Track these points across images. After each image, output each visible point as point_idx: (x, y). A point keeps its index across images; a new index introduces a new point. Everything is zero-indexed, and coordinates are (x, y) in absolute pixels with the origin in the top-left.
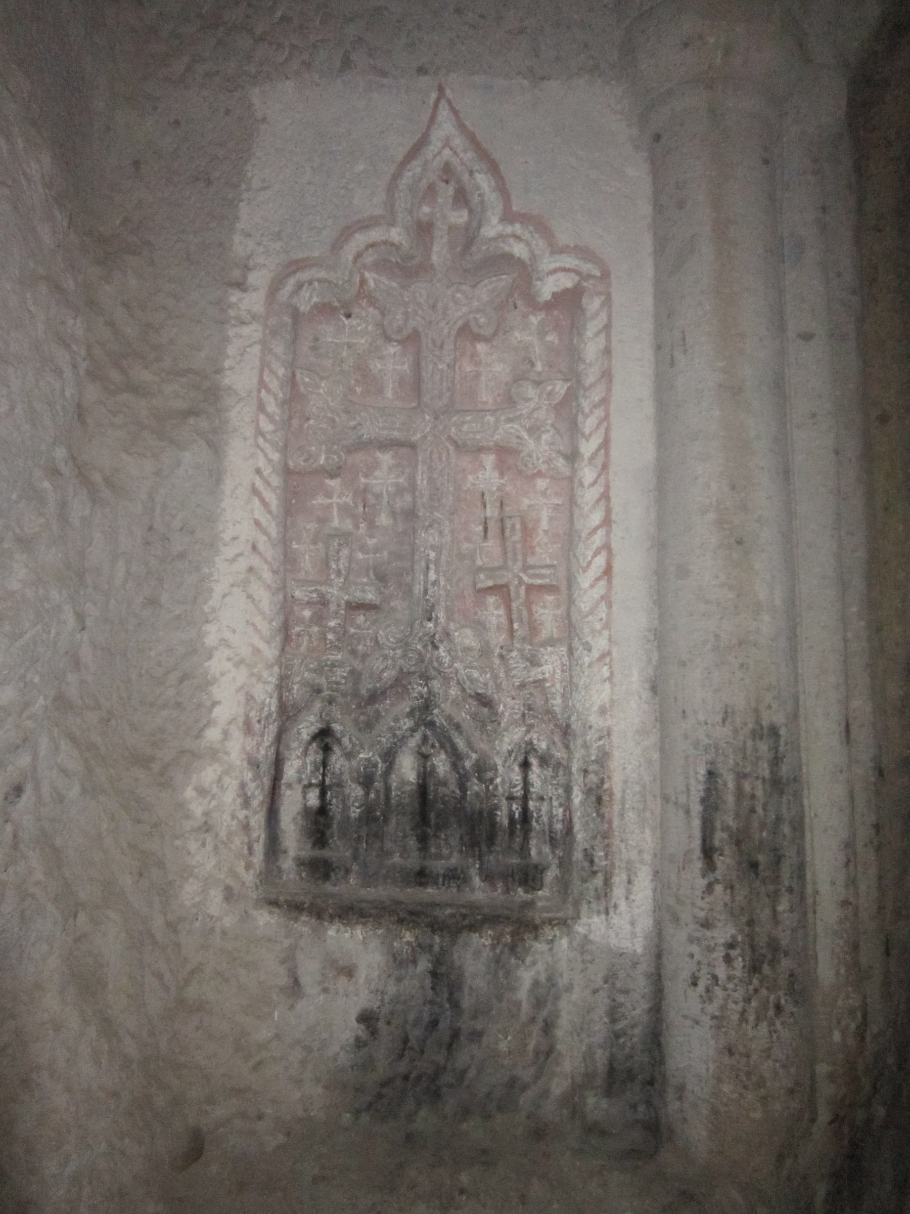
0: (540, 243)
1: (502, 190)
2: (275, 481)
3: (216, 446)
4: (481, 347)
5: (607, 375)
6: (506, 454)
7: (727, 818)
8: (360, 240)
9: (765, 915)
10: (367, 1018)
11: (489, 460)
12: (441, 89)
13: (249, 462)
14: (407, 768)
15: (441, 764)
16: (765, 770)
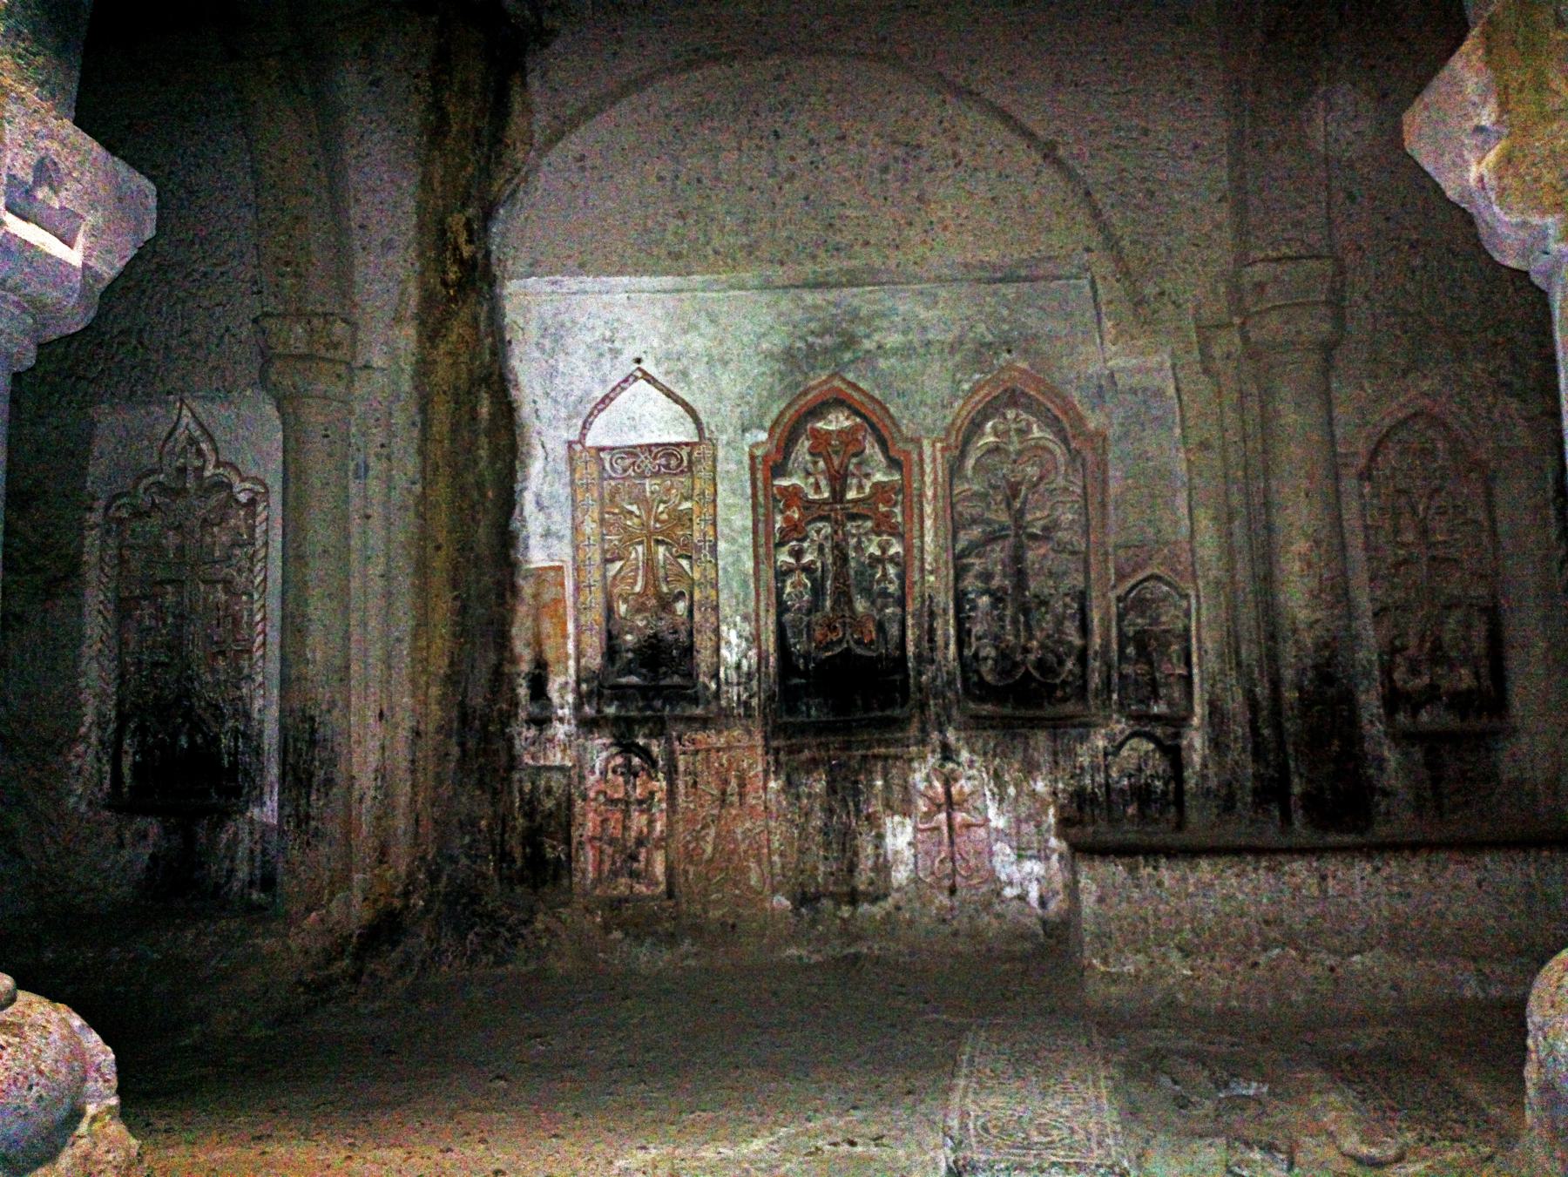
0: (235, 479)
1: (216, 450)
2: (111, 607)
3: (77, 595)
4: (216, 529)
5: (266, 544)
6: (228, 583)
7: (291, 760)
8: (145, 482)
9: (303, 802)
10: (153, 857)
11: (219, 587)
12: (182, 401)
13: (96, 597)
14: (184, 742)
15: (199, 739)
16: (307, 736)
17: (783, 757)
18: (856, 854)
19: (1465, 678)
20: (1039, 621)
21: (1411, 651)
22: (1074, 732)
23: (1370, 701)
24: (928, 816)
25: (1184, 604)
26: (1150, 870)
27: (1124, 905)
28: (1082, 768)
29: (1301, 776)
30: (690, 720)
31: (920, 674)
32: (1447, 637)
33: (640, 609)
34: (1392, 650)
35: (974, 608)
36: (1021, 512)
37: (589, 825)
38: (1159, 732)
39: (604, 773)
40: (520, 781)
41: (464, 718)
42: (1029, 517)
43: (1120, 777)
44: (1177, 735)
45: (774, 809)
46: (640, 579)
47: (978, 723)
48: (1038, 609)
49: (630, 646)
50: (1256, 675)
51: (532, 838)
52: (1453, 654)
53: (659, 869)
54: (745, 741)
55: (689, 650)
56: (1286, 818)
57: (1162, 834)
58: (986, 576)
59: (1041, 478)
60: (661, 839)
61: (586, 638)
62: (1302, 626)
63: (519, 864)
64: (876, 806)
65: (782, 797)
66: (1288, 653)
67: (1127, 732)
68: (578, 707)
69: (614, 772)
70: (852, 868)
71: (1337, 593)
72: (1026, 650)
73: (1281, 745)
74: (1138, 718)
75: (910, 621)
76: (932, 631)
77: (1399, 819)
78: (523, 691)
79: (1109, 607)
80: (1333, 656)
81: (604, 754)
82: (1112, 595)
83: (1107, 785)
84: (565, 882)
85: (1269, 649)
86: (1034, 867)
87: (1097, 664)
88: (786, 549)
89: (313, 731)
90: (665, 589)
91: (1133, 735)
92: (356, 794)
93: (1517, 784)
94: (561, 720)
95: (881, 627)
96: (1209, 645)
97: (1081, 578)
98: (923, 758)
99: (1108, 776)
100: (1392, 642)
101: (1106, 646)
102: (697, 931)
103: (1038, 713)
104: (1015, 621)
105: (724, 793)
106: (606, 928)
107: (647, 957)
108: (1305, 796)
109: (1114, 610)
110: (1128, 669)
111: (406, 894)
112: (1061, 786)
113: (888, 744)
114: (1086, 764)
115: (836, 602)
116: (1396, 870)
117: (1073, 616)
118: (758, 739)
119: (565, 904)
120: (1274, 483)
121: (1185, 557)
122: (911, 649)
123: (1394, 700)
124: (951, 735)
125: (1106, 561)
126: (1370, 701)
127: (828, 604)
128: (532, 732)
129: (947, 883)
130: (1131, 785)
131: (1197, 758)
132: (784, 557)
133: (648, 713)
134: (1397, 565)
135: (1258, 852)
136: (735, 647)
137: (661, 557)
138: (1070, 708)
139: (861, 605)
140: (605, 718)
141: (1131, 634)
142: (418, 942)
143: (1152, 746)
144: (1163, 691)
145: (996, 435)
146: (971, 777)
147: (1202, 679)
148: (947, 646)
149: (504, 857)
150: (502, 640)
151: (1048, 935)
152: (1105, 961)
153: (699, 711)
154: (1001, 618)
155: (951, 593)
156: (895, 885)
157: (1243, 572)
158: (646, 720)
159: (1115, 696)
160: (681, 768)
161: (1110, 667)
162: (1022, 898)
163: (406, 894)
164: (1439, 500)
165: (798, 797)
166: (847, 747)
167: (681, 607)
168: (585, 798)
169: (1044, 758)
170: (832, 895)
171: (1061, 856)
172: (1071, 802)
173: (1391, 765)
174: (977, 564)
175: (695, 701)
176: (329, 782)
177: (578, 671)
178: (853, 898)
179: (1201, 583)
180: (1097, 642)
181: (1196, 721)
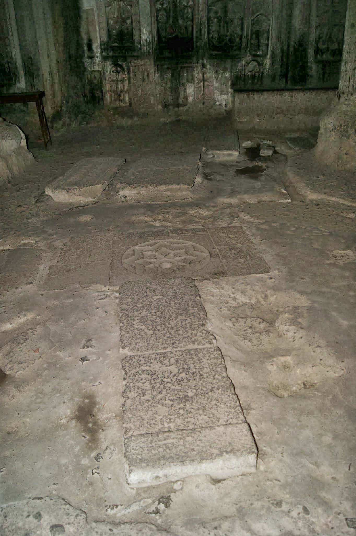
7: (27, 69)
17: (159, 67)
18: (179, 94)
23: (311, 52)
24: (198, 83)
30: (134, 56)
31: (197, 42)
33: (116, 22)
34: (320, 38)
35: (212, 23)
37: (107, 87)
39: (110, 73)
40: (87, 75)
41: (70, 57)
44: (263, 61)
45: (157, 82)
46: (116, 13)
47: (211, 57)
49: (114, 34)
51: (92, 91)
53: (127, 99)
54: (149, 63)
55: (132, 35)
56: (287, 82)
57: (257, 87)
58: (216, 12)
60: (127, 91)
61: (102, 31)
63: (89, 98)
64: (184, 81)
65: (159, 78)
66: (293, 37)
68: (101, 53)
69: (113, 72)
70: (178, 98)
71: (307, 20)
72: (226, 36)
73: (288, 63)
75: (195, 27)
76: (201, 30)
78: (86, 48)
81: (110, 67)
82: (250, 19)
83: (244, 74)
84: (102, 103)
86: (224, 97)
88: (159, 3)
89: (32, 61)
90: (124, 16)
91: (252, 60)
92: (45, 79)
94: (97, 57)
95: (186, 28)
97: (242, 14)
98: (197, 67)
99: (245, 72)
101: (247, 36)
102: (137, 114)
104: (224, 27)
105: (143, 78)
106: (114, 115)
107: (126, 122)
108: (292, 77)
110: (252, 42)
111: (61, 107)
113: (187, 63)
115: (173, 20)
118: (153, 63)
119: (103, 109)
122: (195, 35)
123: (317, 51)
124: (205, 61)
126: (311, 52)
127: (171, 20)
128: (90, 61)
129: (202, 101)
132: (158, 6)
133: (122, 55)
135: (278, 90)
136: (145, 35)
137: (122, 6)
139: (180, 22)
140: (109, 56)
142: (66, 119)
143: (256, 64)
144: (261, 48)
146: (210, 73)
148: (205, 35)
149: (85, 96)
150: (78, 32)
151: (227, 114)
152: (240, 118)
153: (135, 54)
154: (220, 26)
155: (206, 18)
156: (189, 101)
158: (122, 57)
159: (248, 49)
160: (131, 70)
162: (221, 105)
163: (61, 107)
165: (163, 79)
166: (177, 63)
167: (129, 22)
168: (105, 80)
169: (228, 66)
170: (172, 105)
171: (231, 94)
173: (314, 69)
174: (214, 8)
175: (134, 51)
176: (38, 75)
177: (101, 42)
178: (178, 105)
180: (245, 34)
181: (268, 57)
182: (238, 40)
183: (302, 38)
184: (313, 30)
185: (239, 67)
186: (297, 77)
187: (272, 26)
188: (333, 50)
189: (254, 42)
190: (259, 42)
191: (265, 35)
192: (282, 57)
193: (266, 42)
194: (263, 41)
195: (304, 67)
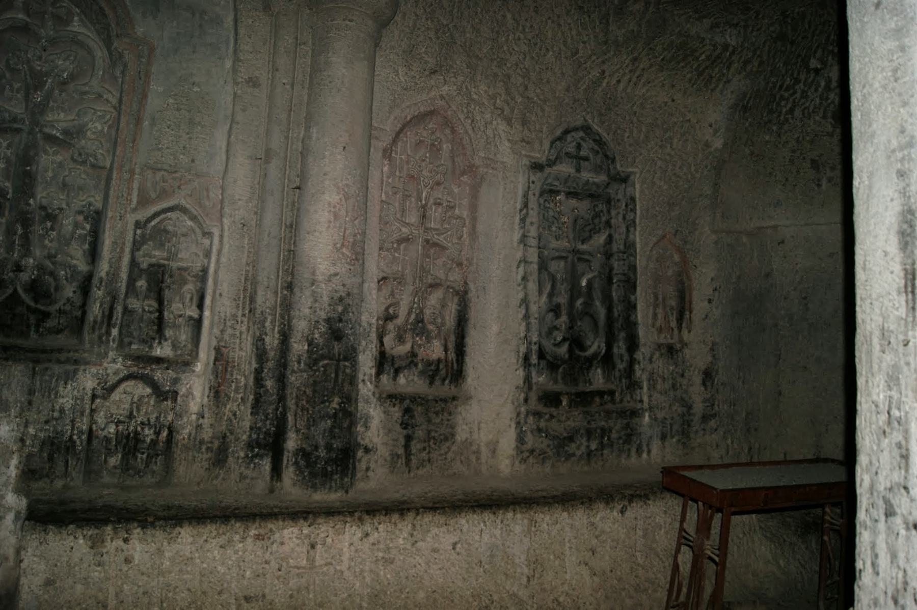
19: (435, 350)
20: (42, 237)
21: (400, 321)
22: (57, 369)
23: (366, 362)
25: (207, 242)
26: (120, 543)
27: (79, 588)
28: (62, 410)
29: (298, 431)
32: (427, 312)
36: (42, 108)
38: (158, 375)
42: (50, 117)
43: (107, 424)
44: (176, 381)
48: (42, 222)
50: (268, 324)
52: (431, 327)
56: (277, 471)
57: (143, 493)
59: (73, 77)
62: (320, 278)
67: (122, 375)
72: (18, 268)
73: (282, 398)
74: (138, 359)
77: (375, 476)
79: (123, 233)
80: (346, 311)
82: (131, 219)
83: (91, 431)
85: (284, 298)
87: (100, 293)
93: (468, 443)
96: (224, 288)
99: (92, 421)
100: (387, 309)
101: (113, 276)
103: (19, 342)
109: (130, 237)
110: (134, 304)
112: (31, 431)
114: (68, 406)
116: (383, 534)
117: (82, 238)
120: (314, 130)
121: (215, 194)
123: (383, 361)
125: (131, 180)
126: (366, 362)
130: (118, 432)
131: (194, 407)
134: (400, 241)
138: (62, 340)
141: (144, 266)
143: (149, 390)
144: (168, 333)
145: (29, 16)
147: (211, 328)
157: (270, 218)
159: (115, 332)
161: (114, 299)
164: (438, 194)
172: (41, 450)
173: (376, 425)
179: (226, 221)
180: (104, 268)
181: (199, 367)
182: (69, 291)
183: (340, 309)
184: (371, 286)
185: (66, 401)
186: (322, 453)
187: (219, 252)
188: (429, 363)
189: (142, 305)
190: (160, 311)
191: (190, 287)
192: (258, 372)
193: (196, 316)
194: (180, 307)
195: (347, 416)
